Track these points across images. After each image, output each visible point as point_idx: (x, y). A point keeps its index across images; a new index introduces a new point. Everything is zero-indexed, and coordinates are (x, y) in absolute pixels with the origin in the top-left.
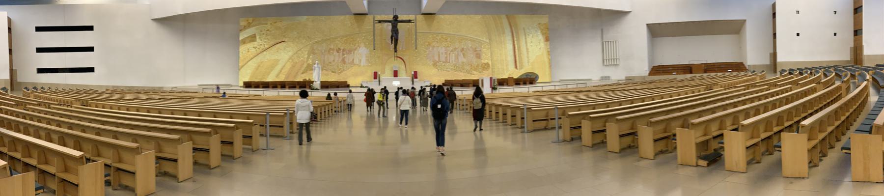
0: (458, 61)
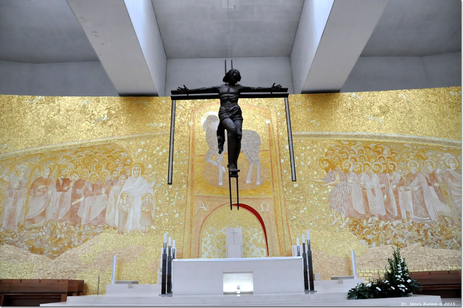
0: (427, 211)
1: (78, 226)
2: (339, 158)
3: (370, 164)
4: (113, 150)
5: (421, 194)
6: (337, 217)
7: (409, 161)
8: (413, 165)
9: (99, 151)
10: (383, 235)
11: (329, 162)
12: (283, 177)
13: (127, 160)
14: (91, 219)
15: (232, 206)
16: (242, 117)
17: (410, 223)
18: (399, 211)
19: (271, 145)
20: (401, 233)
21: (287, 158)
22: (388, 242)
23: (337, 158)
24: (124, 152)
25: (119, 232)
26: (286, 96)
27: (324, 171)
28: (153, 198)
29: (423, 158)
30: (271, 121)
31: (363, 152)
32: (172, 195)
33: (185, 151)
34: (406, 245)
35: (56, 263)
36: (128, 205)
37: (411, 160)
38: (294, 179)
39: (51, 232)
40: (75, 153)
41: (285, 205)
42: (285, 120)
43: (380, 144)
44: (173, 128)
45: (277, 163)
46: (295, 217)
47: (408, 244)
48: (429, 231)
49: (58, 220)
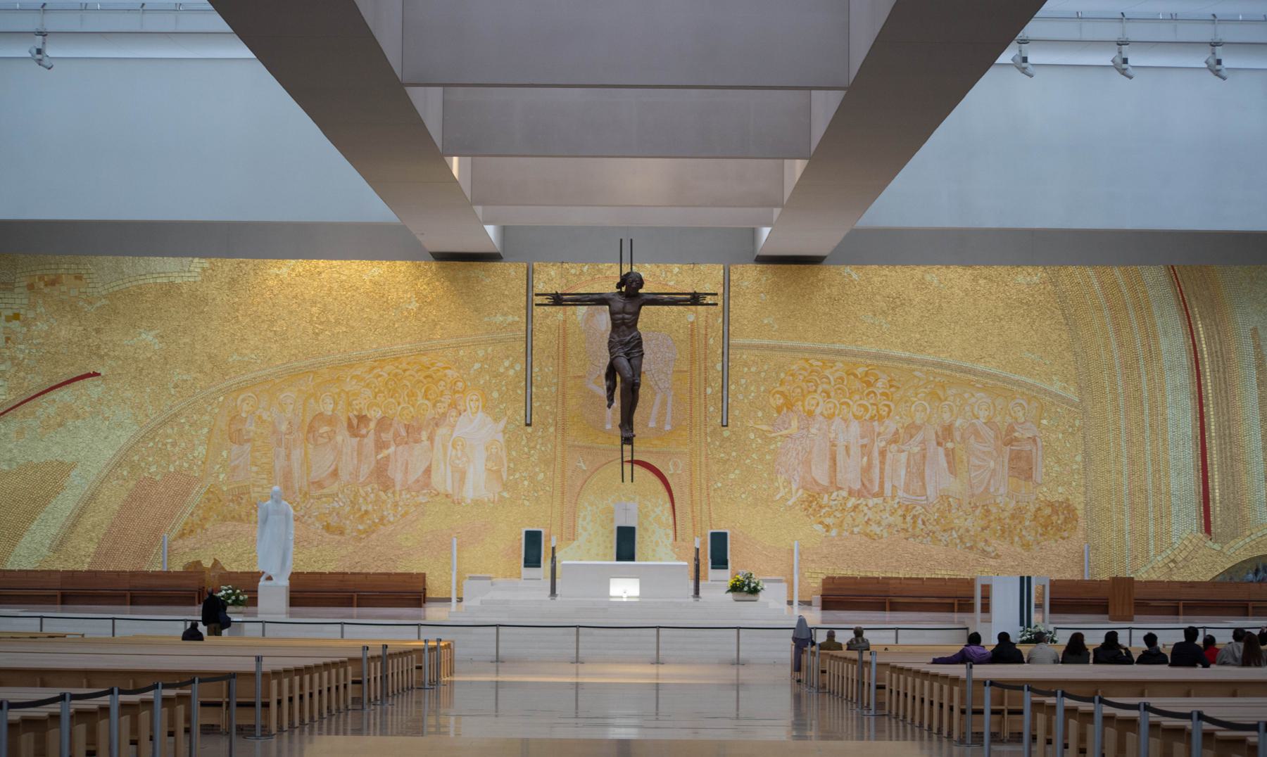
2: (802, 390)
3: (851, 403)
4: (432, 364)
6: (784, 486)
7: (915, 401)
8: (920, 408)
9: (409, 367)
10: (851, 519)
12: (708, 419)
14: (409, 483)
15: (624, 463)
16: (642, 351)
19: (692, 363)
20: (879, 518)
23: (799, 390)
24: (450, 368)
25: (453, 502)
27: (775, 412)
28: (504, 449)
29: (940, 399)
30: (697, 318)
31: (843, 381)
32: (532, 445)
33: (551, 368)
34: (882, 535)
37: (919, 400)
38: (725, 424)
39: (351, 502)
41: (707, 466)
42: (721, 315)
43: (874, 369)
44: (530, 327)
45: (700, 394)
46: (719, 485)
47: (885, 535)
48: (922, 516)
49: (360, 483)
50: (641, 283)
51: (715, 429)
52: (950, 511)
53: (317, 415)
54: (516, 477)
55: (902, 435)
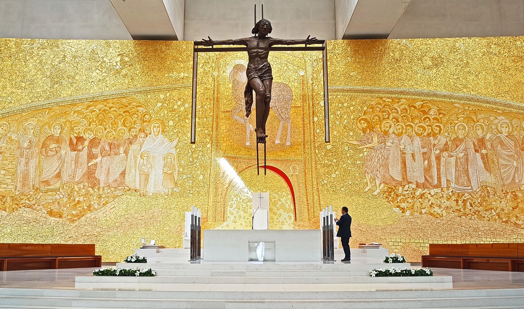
0: (469, 180)
1: (97, 188)
2: (379, 118)
3: (413, 125)
5: (466, 161)
8: (461, 128)
9: (114, 106)
11: (368, 122)
13: (146, 116)
14: (110, 181)
17: (449, 192)
18: (439, 179)
19: (304, 101)
20: (439, 202)
21: (321, 116)
22: (423, 211)
23: (377, 118)
24: (141, 106)
26: (322, 49)
27: (362, 132)
29: (474, 121)
30: (306, 72)
32: (195, 156)
33: (209, 106)
34: (442, 215)
35: (77, 227)
36: (149, 166)
38: (327, 140)
39: (69, 195)
40: (87, 108)
41: (316, 169)
42: (322, 71)
45: (310, 121)
46: (326, 182)
50: (270, 32)
51: (320, 144)
52: (489, 197)
53: (49, 136)
54: (184, 178)
55: (450, 146)
